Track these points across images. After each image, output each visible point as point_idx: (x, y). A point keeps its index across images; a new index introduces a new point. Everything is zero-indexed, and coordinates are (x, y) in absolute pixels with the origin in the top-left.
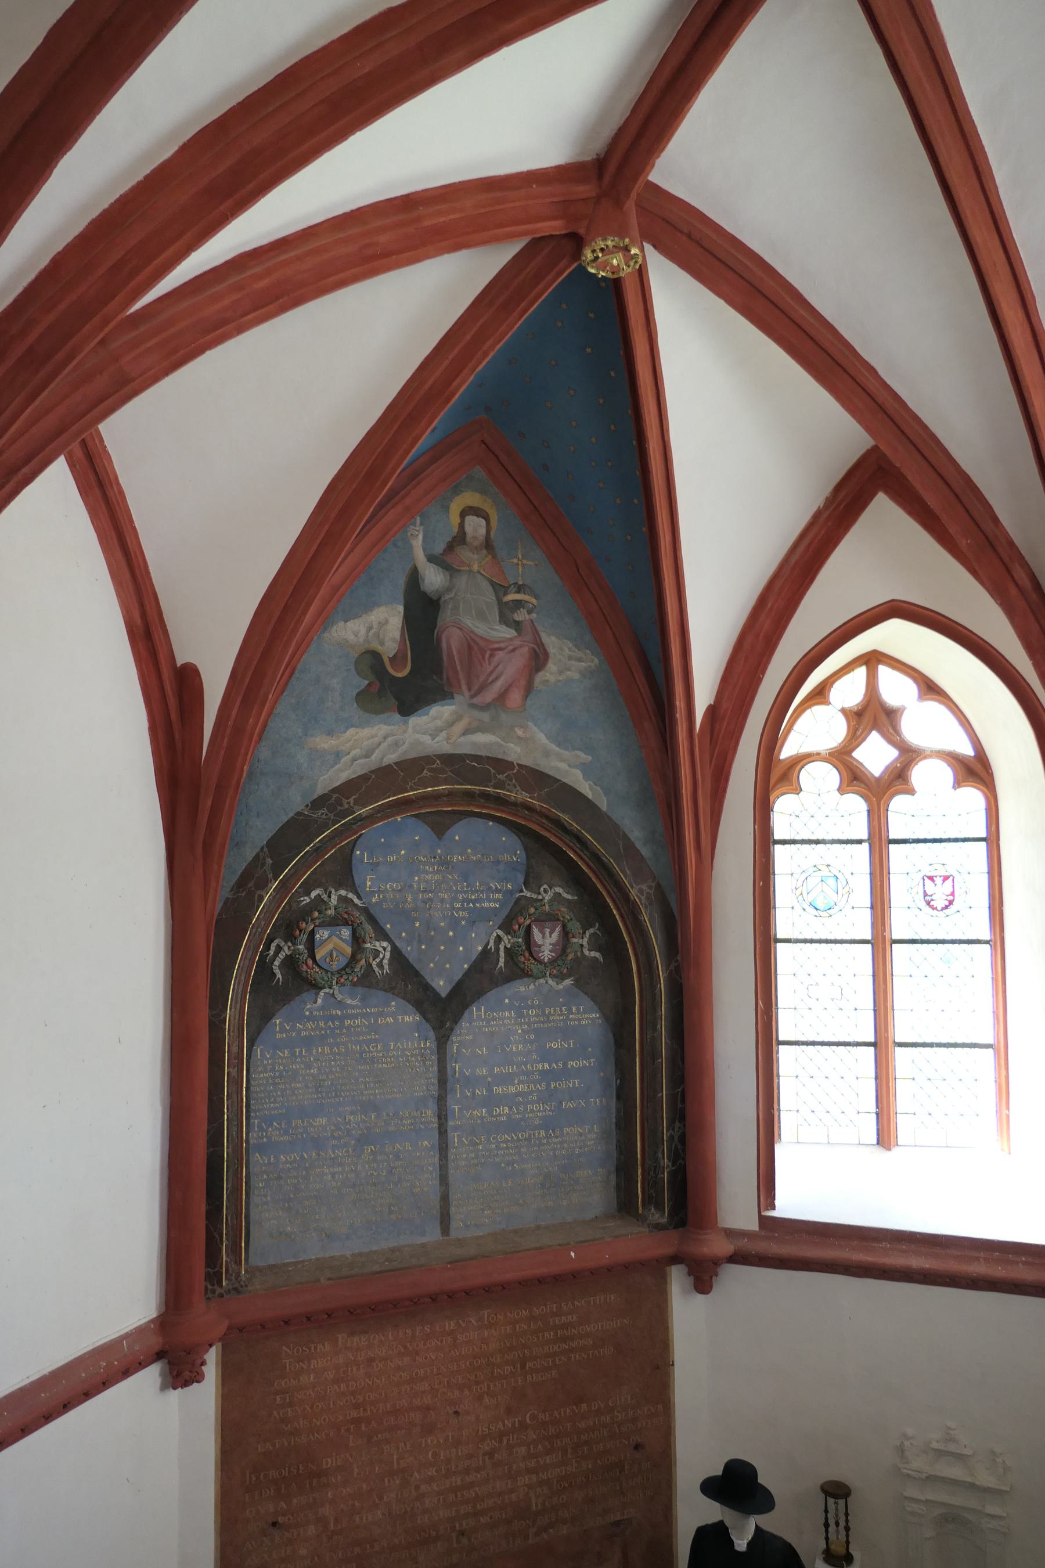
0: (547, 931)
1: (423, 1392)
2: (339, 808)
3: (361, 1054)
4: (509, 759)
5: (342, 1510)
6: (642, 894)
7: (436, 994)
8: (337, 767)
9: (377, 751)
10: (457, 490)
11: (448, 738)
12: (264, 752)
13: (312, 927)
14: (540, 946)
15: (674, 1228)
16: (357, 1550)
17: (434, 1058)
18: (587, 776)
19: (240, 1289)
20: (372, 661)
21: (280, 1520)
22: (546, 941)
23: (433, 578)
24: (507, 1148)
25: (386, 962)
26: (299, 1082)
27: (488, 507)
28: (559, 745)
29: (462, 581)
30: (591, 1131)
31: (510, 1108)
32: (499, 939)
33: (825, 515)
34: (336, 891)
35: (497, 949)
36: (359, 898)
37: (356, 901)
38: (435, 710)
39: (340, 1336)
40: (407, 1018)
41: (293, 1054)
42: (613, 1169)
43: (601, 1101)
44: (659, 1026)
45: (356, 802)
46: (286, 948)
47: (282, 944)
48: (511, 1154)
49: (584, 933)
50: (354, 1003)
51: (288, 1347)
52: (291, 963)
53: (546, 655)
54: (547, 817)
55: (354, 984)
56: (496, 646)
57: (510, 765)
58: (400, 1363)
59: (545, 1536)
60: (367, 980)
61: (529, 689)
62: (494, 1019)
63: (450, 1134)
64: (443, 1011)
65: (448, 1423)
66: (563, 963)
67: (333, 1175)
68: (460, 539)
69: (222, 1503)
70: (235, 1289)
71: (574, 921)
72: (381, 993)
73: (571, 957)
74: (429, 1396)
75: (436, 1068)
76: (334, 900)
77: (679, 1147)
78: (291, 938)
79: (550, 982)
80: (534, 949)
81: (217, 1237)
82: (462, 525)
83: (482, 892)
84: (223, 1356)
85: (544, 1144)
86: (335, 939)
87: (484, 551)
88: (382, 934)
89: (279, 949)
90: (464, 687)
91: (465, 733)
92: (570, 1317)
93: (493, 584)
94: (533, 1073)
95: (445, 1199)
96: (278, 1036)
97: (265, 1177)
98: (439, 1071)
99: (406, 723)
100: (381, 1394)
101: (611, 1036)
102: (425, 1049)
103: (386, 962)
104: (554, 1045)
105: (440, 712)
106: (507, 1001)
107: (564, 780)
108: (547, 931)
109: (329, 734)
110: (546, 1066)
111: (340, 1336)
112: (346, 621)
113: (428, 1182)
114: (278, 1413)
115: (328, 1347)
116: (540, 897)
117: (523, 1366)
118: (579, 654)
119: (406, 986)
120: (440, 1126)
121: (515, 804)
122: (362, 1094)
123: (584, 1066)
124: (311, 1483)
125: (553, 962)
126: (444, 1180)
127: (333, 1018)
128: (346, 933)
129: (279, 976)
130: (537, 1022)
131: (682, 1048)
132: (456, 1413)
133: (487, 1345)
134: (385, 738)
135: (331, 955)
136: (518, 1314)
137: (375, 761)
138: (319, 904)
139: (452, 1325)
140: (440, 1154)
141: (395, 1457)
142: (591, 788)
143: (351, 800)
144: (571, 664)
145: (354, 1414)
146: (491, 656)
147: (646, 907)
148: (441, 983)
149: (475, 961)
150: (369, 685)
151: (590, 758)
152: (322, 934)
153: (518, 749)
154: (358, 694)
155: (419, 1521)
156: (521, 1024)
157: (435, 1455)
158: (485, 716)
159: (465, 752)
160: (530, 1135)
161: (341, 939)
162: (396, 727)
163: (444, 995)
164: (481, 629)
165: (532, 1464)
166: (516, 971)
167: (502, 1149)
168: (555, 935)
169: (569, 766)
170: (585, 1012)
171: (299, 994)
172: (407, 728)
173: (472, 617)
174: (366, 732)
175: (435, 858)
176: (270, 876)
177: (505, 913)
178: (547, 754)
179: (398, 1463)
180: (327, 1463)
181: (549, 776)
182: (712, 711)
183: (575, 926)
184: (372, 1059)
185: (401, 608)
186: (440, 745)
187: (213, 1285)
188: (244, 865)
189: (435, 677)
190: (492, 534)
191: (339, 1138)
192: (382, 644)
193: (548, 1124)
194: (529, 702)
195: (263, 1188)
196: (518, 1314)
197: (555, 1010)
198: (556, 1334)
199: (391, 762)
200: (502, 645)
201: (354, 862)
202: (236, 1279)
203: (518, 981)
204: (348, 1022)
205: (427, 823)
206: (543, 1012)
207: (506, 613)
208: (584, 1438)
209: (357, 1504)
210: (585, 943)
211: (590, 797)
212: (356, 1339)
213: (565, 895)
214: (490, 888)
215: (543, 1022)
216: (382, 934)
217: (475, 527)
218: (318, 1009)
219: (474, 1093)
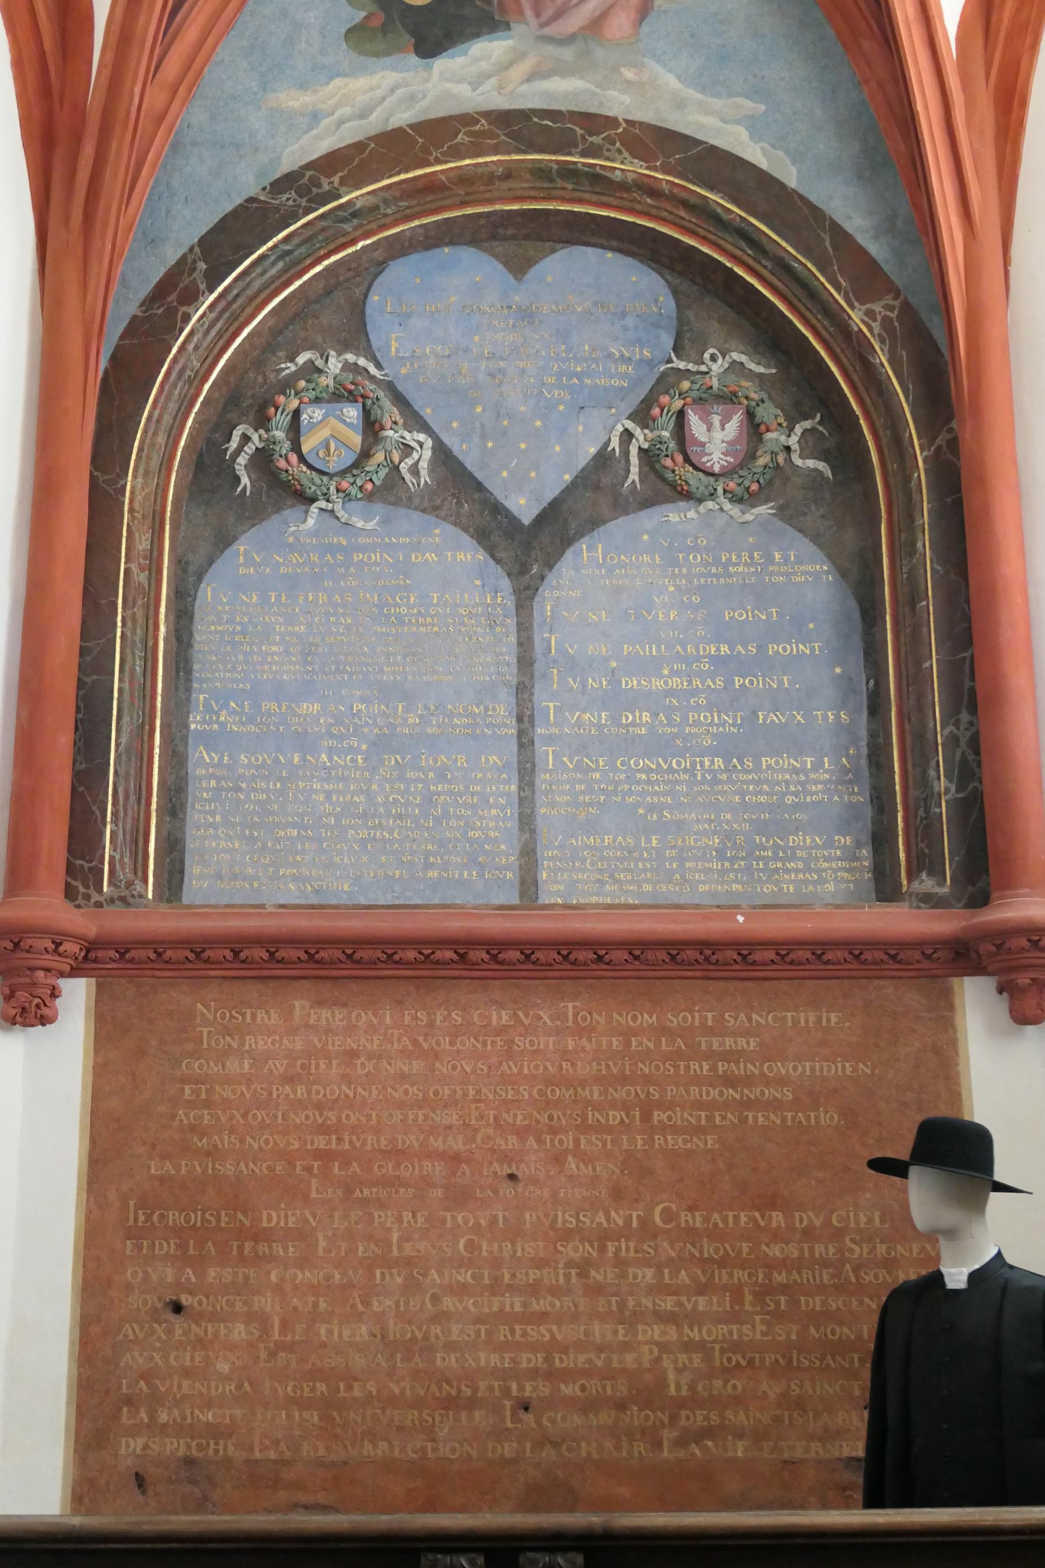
0: (716, 420)
1: (450, 1127)
2: (315, 190)
3: (380, 607)
4: (610, 114)
5: (295, 1309)
6: (875, 320)
7: (513, 520)
8: (314, 132)
9: (379, 110)
11: (500, 88)
12: (196, 115)
13: (295, 403)
14: (703, 445)
15: (967, 906)
16: (321, 1387)
17: (512, 622)
18: (755, 134)
19: (131, 900)
21: (185, 1300)
22: (717, 437)
24: (649, 782)
25: (424, 465)
26: (275, 644)
28: (703, 90)
30: (818, 766)
31: (655, 715)
32: (627, 436)
34: (339, 354)
35: (626, 453)
36: (379, 366)
37: (373, 370)
39: (297, 1004)
40: (461, 556)
41: (265, 599)
42: (866, 838)
43: (837, 717)
44: (919, 545)
45: (343, 182)
46: (255, 437)
47: (250, 432)
48: (656, 793)
49: (791, 430)
50: (370, 525)
51: (207, 1007)
52: (263, 459)
54: (685, 204)
55: (370, 497)
58: (406, 1069)
59: (698, 1453)
60: (390, 491)
62: (622, 565)
63: (540, 748)
64: (527, 546)
65: (496, 1192)
66: (755, 481)
67: (328, 795)
69: (87, 1247)
70: (123, 899)
71: (768, 404)
72: (416, 515)
73: (763, 460)
74: (460, 1137)
75: (513, 639)
76: (334, 365)
77: (971, 757)
78: (262, 422)
79: (727, 506)
80: (692, 450)
81: (97, 812)
83: (596, 361)
84: (97, 1001)
85: (720, 782)
86: (333, 421)
88: (416, 421)
89: (246, 439)
90: (529, 13)
91: (530, 78)
92: (742, 1042)
94: (698, 658)
95: (529, 856)
96: (242, 571)
97: (213, 783)
98: (520, 644)
99: (429, 68)
100: (369, 1117)
101: (853, 604)
102: (494, 606)
103: (424, 465)
104: (740, 616)
105: (486, 51)
106: (646, 537)
108: (716, 420)
109: (301, 88)
110: (724, 649)
111: (297, 1004)
113: (497, 823)
114: (187, 1115)
115: (274, 1019)
116: (703, 368)
117: (646, 1117)
119: (459, 504)
120: (521, 733)
121: (623, 186)
122: (382, 671)
123: (801, 656)
124: (241, 1248)
125: (727, 473)
126: (527, 821)
127: (333, 549)
128: (352, 412)
129: (245, 480)
130: (705, 575)
131: (966, 580)
132: (512, 1177)
133: (573, 1065)
134: (392, 91)
135: (328, 449)
136: (635, 1019)
137: (375, 123)
138: (312, 370)
139: (505, 1017)
140: (521, 780)
141: (395, 1236)
143: (336, 180)
145: (321, 1143)
147: (882, 341)
148: (522, 502)
149: (583, 470)
150: (367, 18)
152: (312, 414)
153: (627, 99)
154: (349, 31)
155: (439, 1362)
156: (674, 576)
157: (470, 1245)
158: (567, 54)
160: (693, 764)
161: (344, 422)
162: (412, 74)
163: (527, 520)
165: (668, 1304)
166: (664, 487)
167: (638, 782)
168: (734, 425)
169: (723, 120)
170: (799, 561)
171: (278, 510)
172: (431, 74)
174: (362, 82)
175: (509, 307)
176: (203, 287)
177: (642, 392)
178: (680, 104)
179: (400, 1248)
180: (270, 1220)
183: (768, 412)
184: (399, 617)
186: (491, 97)
187: (87, 887)
188: (162, 271)
191: (341, 738)
193: (726, 748)
194: (645, 28)
195: (210, 801)
196: (635, 1019)
197: (739, 557)
198: (713, 1068)
201: (368, 311)
202: (127, 888)
203: (666, 507)
204: (357, 557)
205: (496, 257)
206: (717, 562)
208: (780, 1278)
209: (323, 1305)
210: (795, 447)
211: (763, 164)
212: (325, 1013)
213: (752, 366)
214: (610, 355)
215: (717, 576)
216: (416, 421)
218: (311, 533)
219: (584, 684)
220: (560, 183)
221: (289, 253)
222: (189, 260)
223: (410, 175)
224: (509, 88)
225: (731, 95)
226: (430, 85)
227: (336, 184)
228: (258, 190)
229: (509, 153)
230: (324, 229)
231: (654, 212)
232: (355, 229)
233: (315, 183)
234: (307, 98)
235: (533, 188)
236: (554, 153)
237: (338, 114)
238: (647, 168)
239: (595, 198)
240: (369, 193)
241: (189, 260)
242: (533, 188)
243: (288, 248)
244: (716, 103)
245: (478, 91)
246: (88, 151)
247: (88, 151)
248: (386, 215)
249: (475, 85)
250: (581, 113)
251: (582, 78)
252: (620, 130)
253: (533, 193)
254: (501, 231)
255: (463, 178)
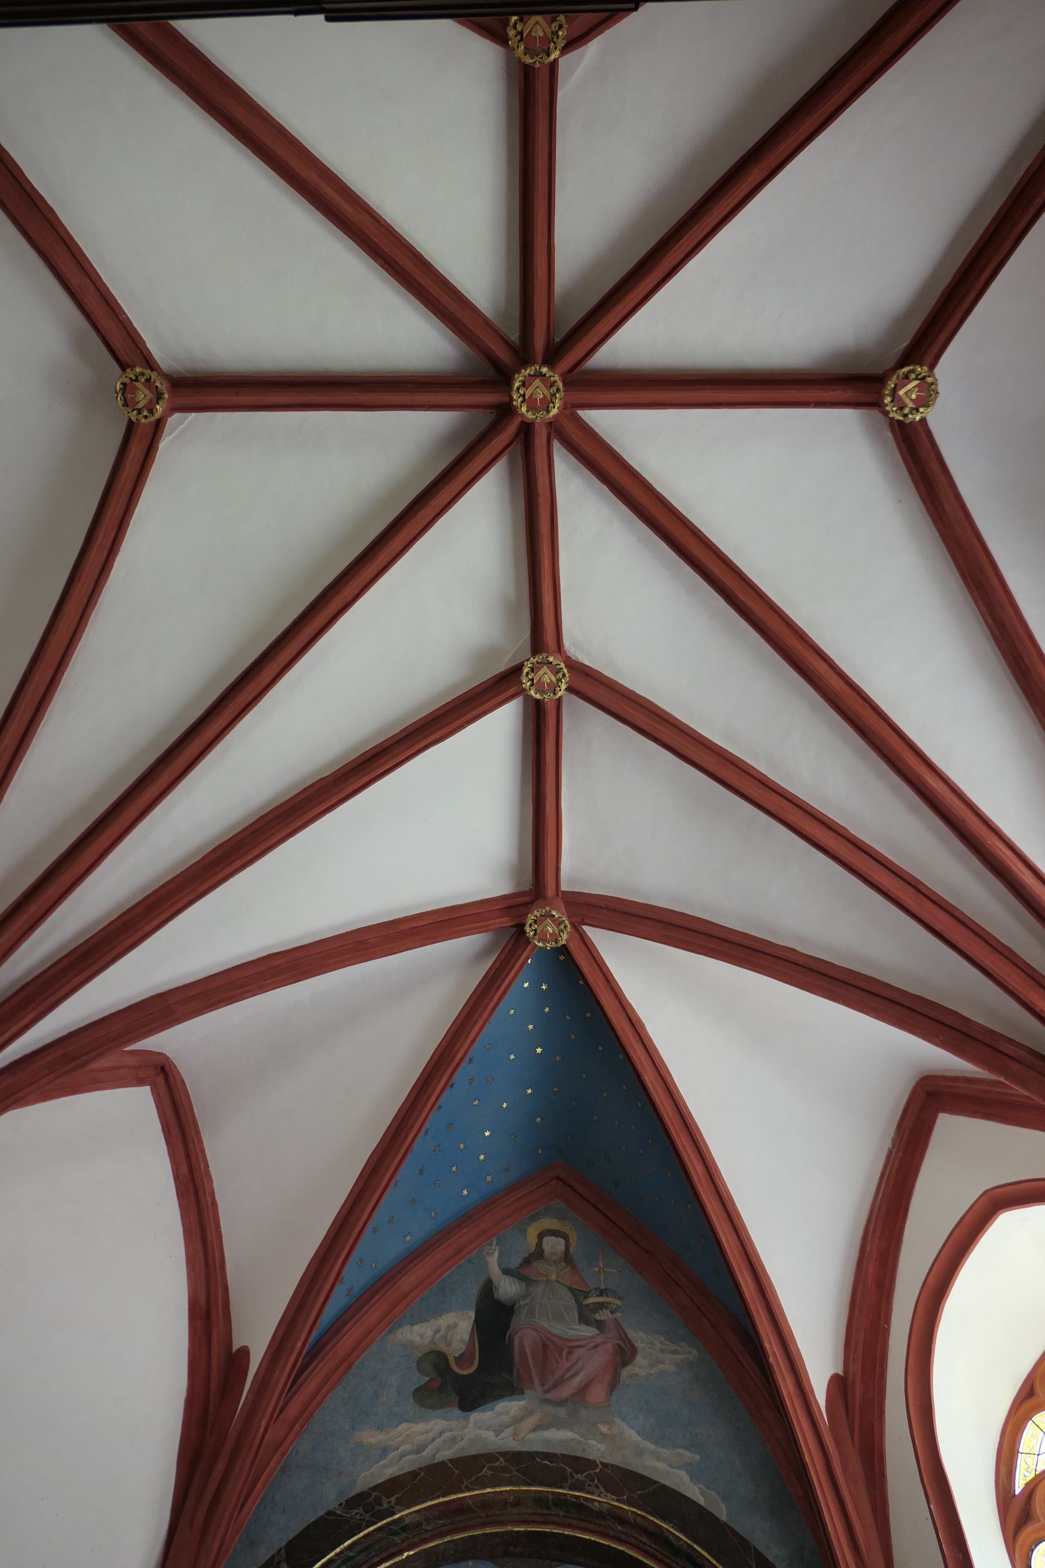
2: (377, 1508)
4: (591, 1458)
8: (382, 1463)
9: (430, 1447)
10: (534, 1218)
11: (515, 1435)
18: (694, 1478)
20: (436, 1361)
23: (507, 1288)
27: (566, 1230)
28: (655, 1443)
29: (539, 1290)
33: (894, 1151)
38: (501, 1405)
45: (398, 1503)
53: (634, 1351)
54: (646, 1531)
56: (575, 1344)
57: (591, 1464)
61: (614, 1384)
68: (538, 1254)
82: (539, 1244)
87: (564, 1264)
90: (536, 1382)
91: (535, 1429)
93: (572, 1290)
99: (467, 1419)
105: (508, 1407)
107: (666, 1483)
112: (413, 1325)
118: (673, 1347)
121: (600, 1515)
134: (441, 1433)
137: (426, 1457)
142: (702, 1493)
143: (393, 1499)
144: (661, 1357)
146: (569, 1353)
151: (698, 1457)
153: (602, 1447)
154: (417, 1390)
158: (562, 1412)
159: (535, 1449)
162: (455, 1422)
164: (558, 1329)
169: (670, 1466)
173: (548, 1316)
174: (420, 1427)
178: (640, 1452)
181: (643, 1477)
182: (839, 1384)
185: (472, 1314)
186: (507, 1441)
189: (503, 1374)
190: (572, 1249)
192: (449, 1344)
194: (614, 1397)
199: (445, 1458)
200: (582, 1343)
207: (585, 1316)
211: (702, 1502)
217: (554, 1245)
220: (554, 1511)
221: (351, 1559)
222: (276, 1561)
223: (447, 1499)
224: (522, 1435)
225: (675, 1447)
226: (466, 1431)
227: (393, 1504)
228: (336, 1505)
229: (518, 1485)
230: (379, 1540)
231: (623, 1537)
232: (403, 1541)
233: (378, 1501)
234: (382, 1437)
235: (535, 1514)
236: (551, 1486)
237: (402, 1448)
238: (617, 1501)
239: (581, 1524)
240: (415, 1512)
241: (276, 1561)
242: (535, 1514)
243: (351, 1554)
244: (665, 1452)
245: (501, 1436)
246: (220, 1466)
247: (220, 1466)
248: (427, 1531)
249: (497, 1433)
250: (569, 1456)
251: (572, 1430)
252: (598, 1470)
253: (536, 1518)
254: (511, 1549)
255: (485, 1503)
